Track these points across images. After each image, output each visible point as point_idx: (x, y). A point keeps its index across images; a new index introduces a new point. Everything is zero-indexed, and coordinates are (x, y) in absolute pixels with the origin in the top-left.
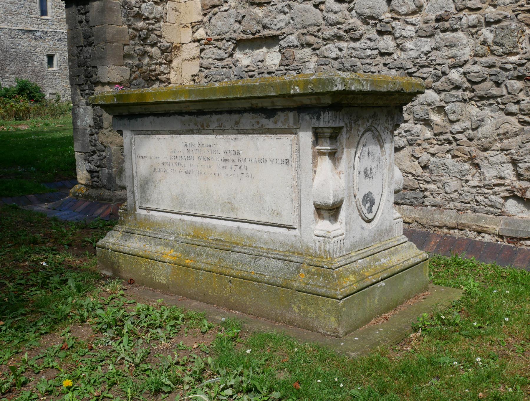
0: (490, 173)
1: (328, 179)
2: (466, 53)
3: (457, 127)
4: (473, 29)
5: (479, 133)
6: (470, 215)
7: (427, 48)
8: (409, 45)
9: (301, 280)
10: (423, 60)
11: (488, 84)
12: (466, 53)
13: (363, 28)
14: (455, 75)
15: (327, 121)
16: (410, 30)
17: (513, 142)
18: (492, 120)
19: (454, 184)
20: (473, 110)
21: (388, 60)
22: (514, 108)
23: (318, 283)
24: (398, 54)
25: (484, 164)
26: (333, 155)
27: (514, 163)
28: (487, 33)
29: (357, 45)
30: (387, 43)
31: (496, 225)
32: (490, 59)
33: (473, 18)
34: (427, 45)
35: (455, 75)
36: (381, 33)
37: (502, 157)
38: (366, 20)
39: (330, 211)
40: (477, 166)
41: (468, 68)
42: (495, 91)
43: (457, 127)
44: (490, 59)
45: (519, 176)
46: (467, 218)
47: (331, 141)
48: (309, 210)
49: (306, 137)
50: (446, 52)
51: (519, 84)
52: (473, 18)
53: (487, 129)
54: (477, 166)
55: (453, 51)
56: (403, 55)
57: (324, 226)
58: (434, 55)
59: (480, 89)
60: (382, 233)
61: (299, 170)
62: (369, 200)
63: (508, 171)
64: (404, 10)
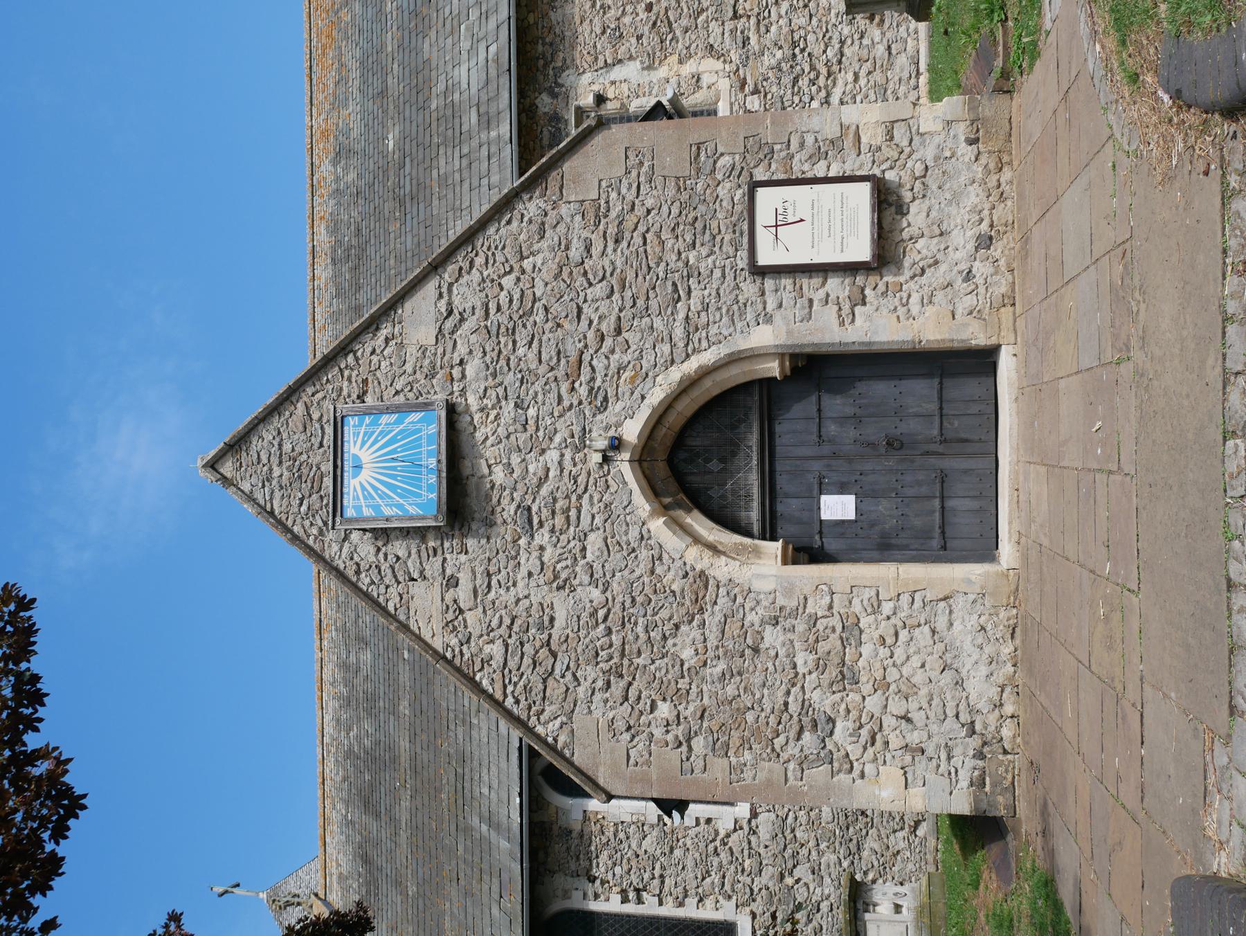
0: (902, 845)
1: (884, 908)
2: (833, 858)
3: (876, 863)
4: (820, 854)
5: (879, 851)
6: (928, 856)
7: (829, 880)
8: (827, 892)
9: (926, 920)
10: (836, 883)
11: (851, 846)
12: (833, 858)
13: (814, 923)
14: (845, 864)
15: (860, 906)
16: (818, 891)
17: (883, 832)
18: (871, 843)
19: (910, 866)
20: (865, 854)
21: (835, 906)
22: (864, 831)
23: (926, 910)
24: (832, 899)
25: (897, 848)
26: (875, 905)
27: (895, 831)
28: (823, 846)
29: (824, 928)
30: (825, 906)
31: (932, 842)
32: (837, 844)
33: (814, 853)
34: (827, 880)
35: (845, 864)
36: (818, 910)
37: (892, 838)
38: (810, 921)
39: (898, 908)
40: (898, 852)
41: (841, 857)
42: (855, 842)
43: (876, 863)
44: (837, 844)
45: (902, 829)
46: (930, 857)
47: (868, 906)
48: (898, 917)
49: (867, 916)
50: (832, 869)
51: (851, 829)
52: (814, 853)
53: (876, 846)
54: (898, 852)
55: (832, 865)
56: (833, 896)
57: (904, 910)
58: (833, 876)
59: (854, 849)
60: (913, 890)
61: (881, 921)
62: (896, 894)
63: (900, 834)
64: (806, 894)
